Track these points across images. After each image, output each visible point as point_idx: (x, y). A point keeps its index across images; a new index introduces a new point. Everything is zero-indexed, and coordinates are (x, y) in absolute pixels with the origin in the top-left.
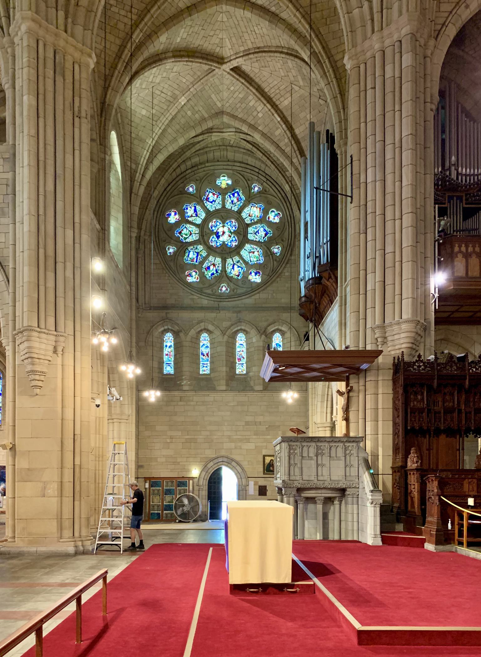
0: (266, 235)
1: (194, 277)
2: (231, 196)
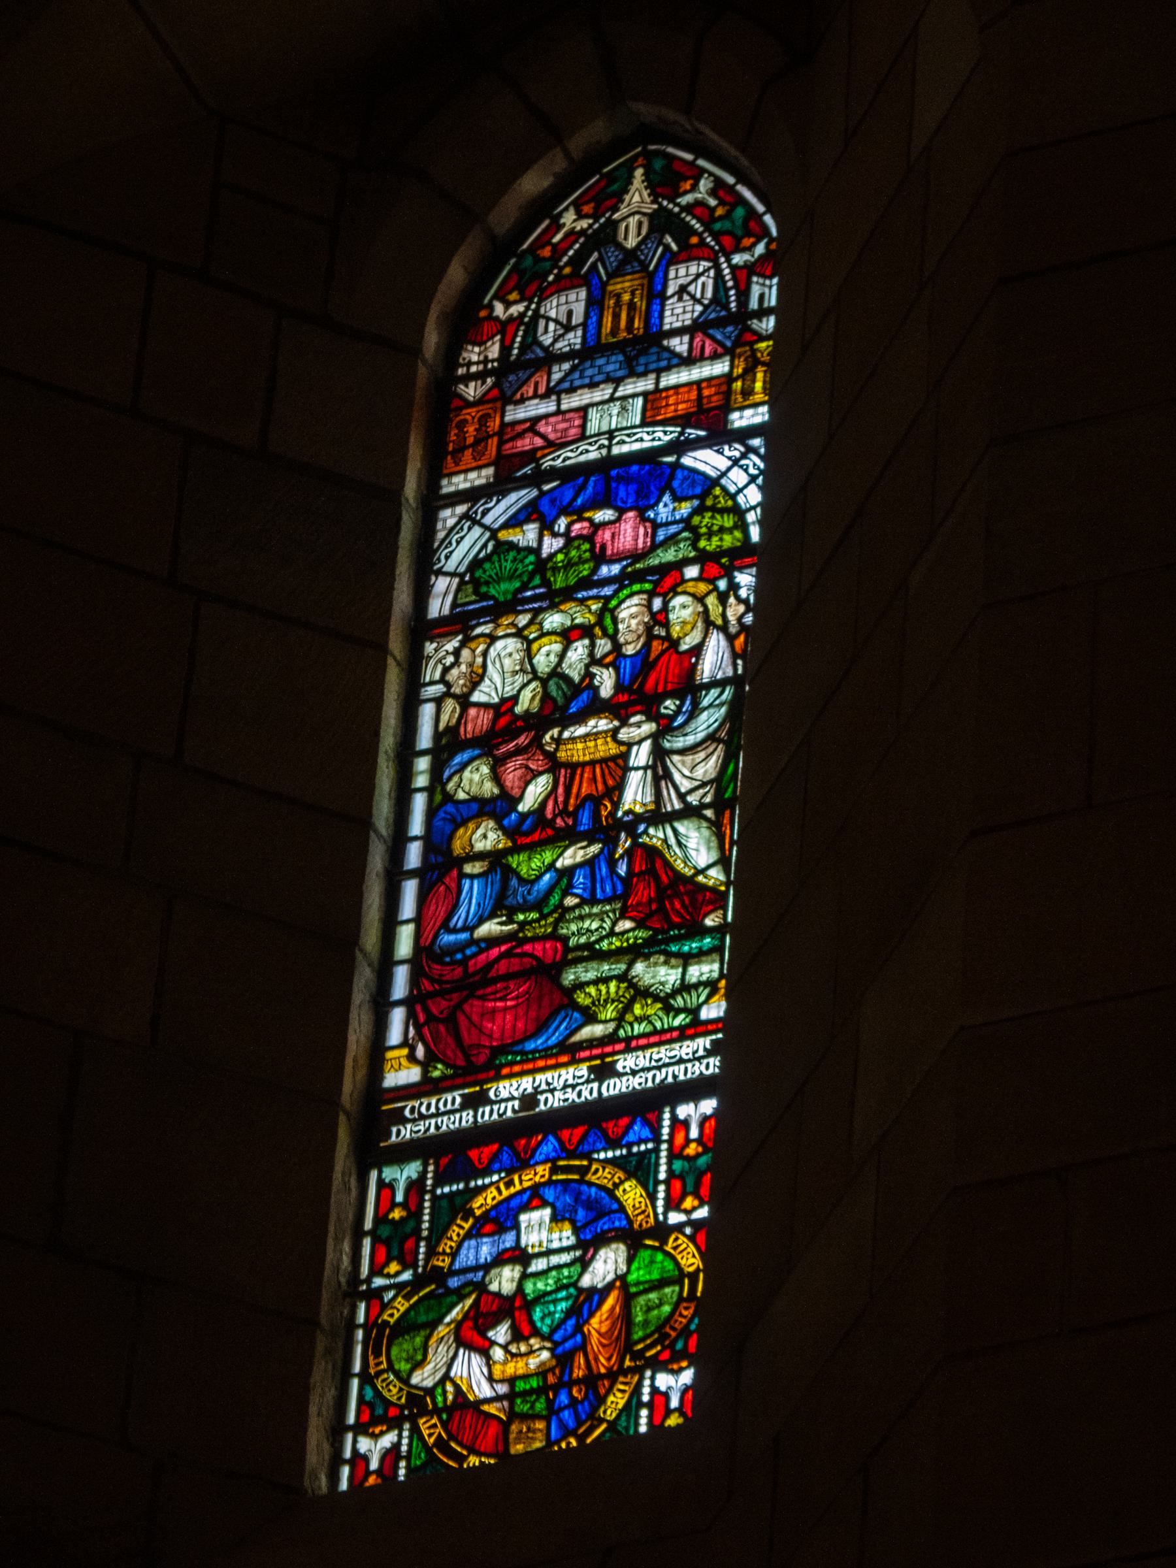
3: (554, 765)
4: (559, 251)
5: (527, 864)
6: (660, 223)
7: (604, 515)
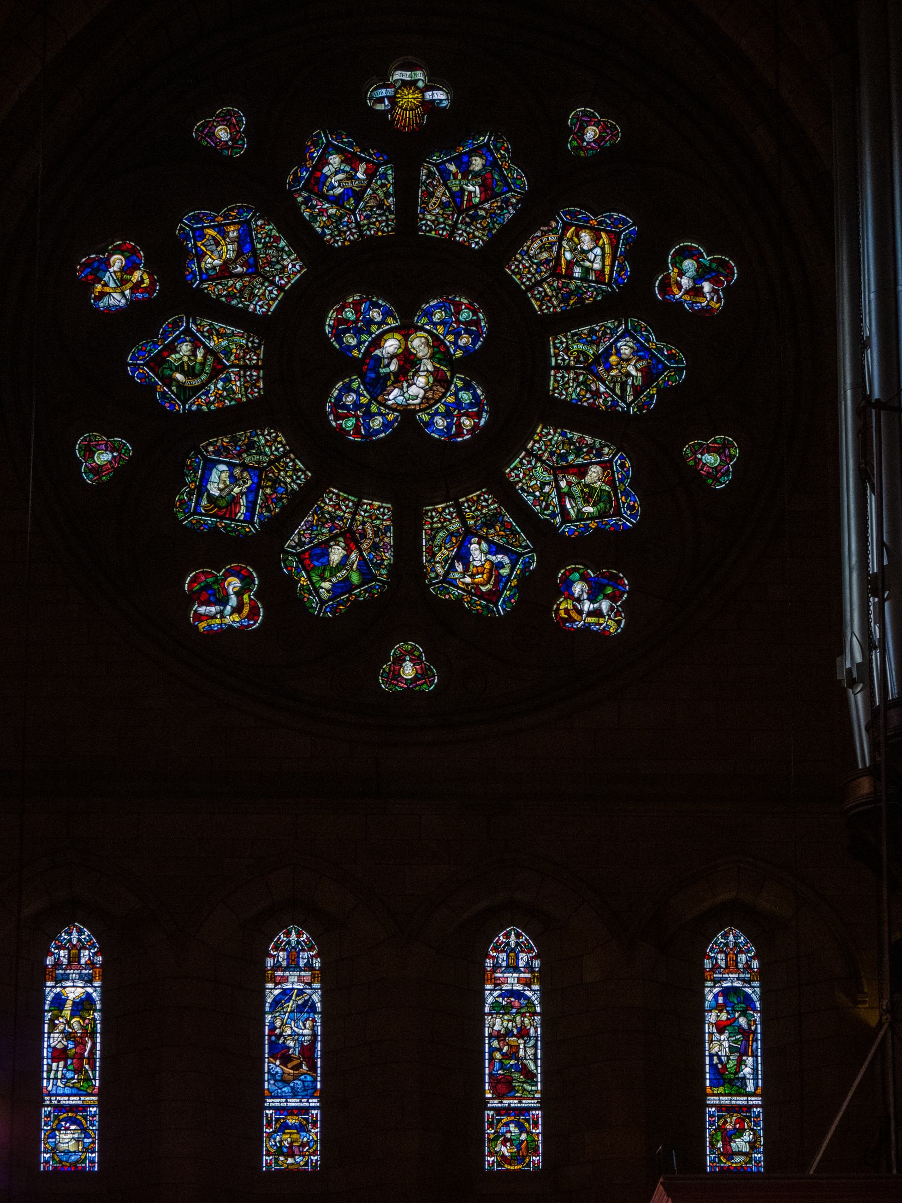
0: (649, 375)
1: (233, 601)
2: (453, 168)
3: (508, 1044)
4: (501, 944)
5: (506, 1062)
6: (517, 944)
7: (513, 999)
